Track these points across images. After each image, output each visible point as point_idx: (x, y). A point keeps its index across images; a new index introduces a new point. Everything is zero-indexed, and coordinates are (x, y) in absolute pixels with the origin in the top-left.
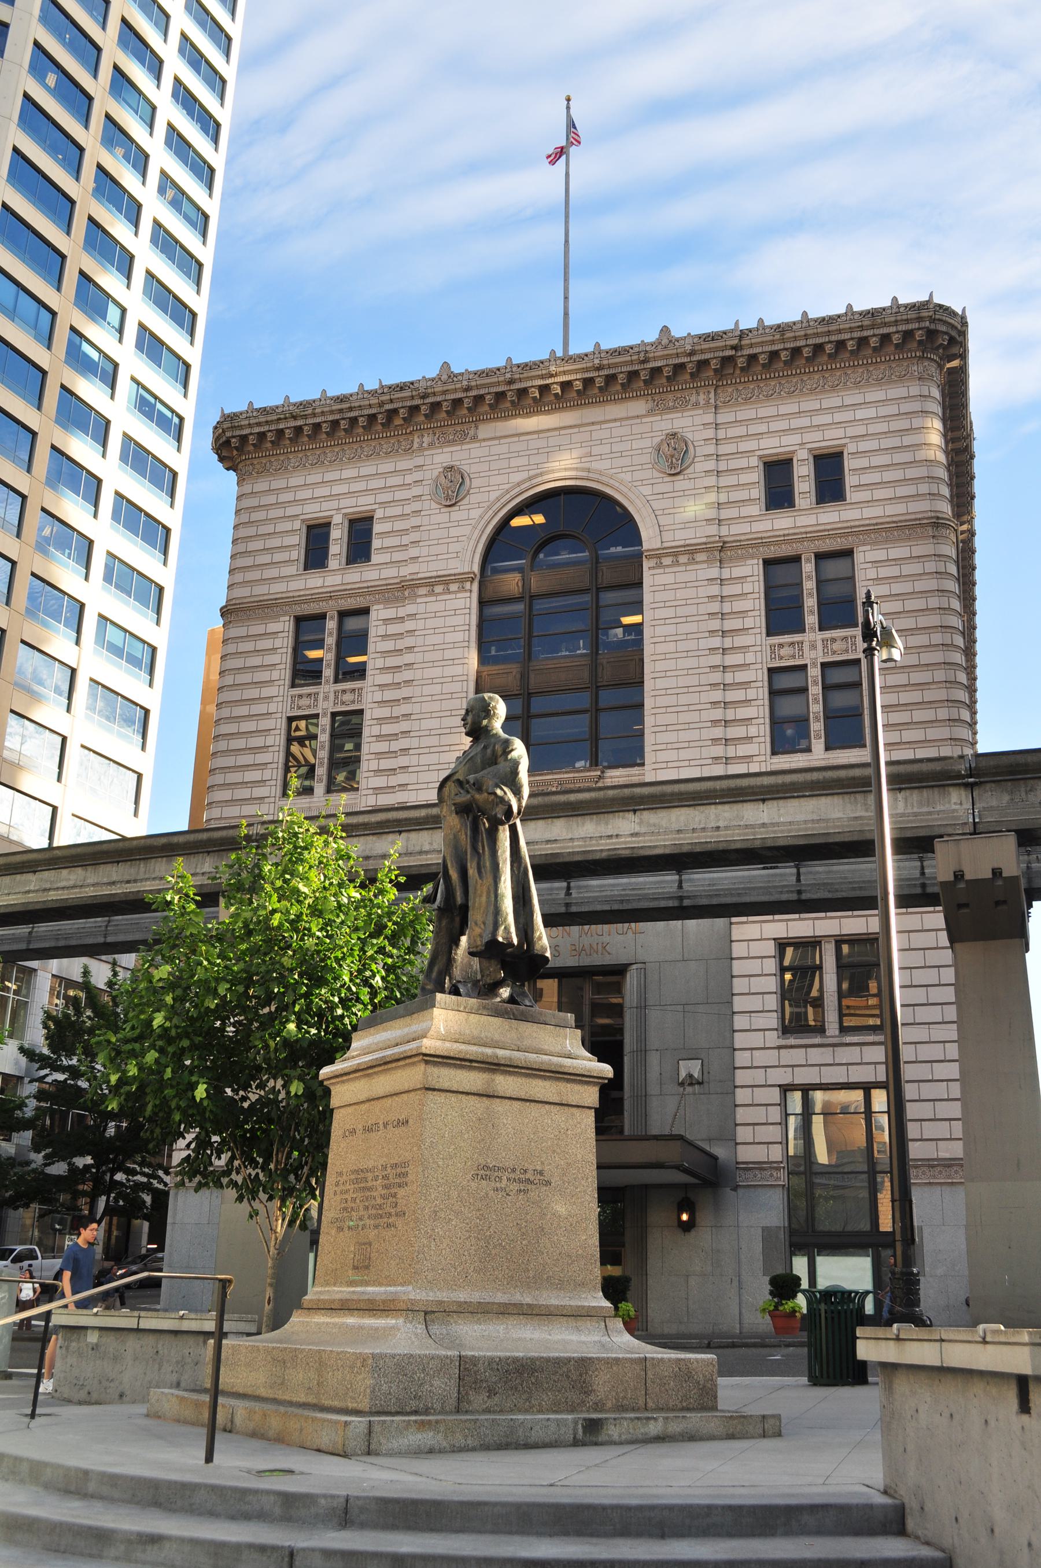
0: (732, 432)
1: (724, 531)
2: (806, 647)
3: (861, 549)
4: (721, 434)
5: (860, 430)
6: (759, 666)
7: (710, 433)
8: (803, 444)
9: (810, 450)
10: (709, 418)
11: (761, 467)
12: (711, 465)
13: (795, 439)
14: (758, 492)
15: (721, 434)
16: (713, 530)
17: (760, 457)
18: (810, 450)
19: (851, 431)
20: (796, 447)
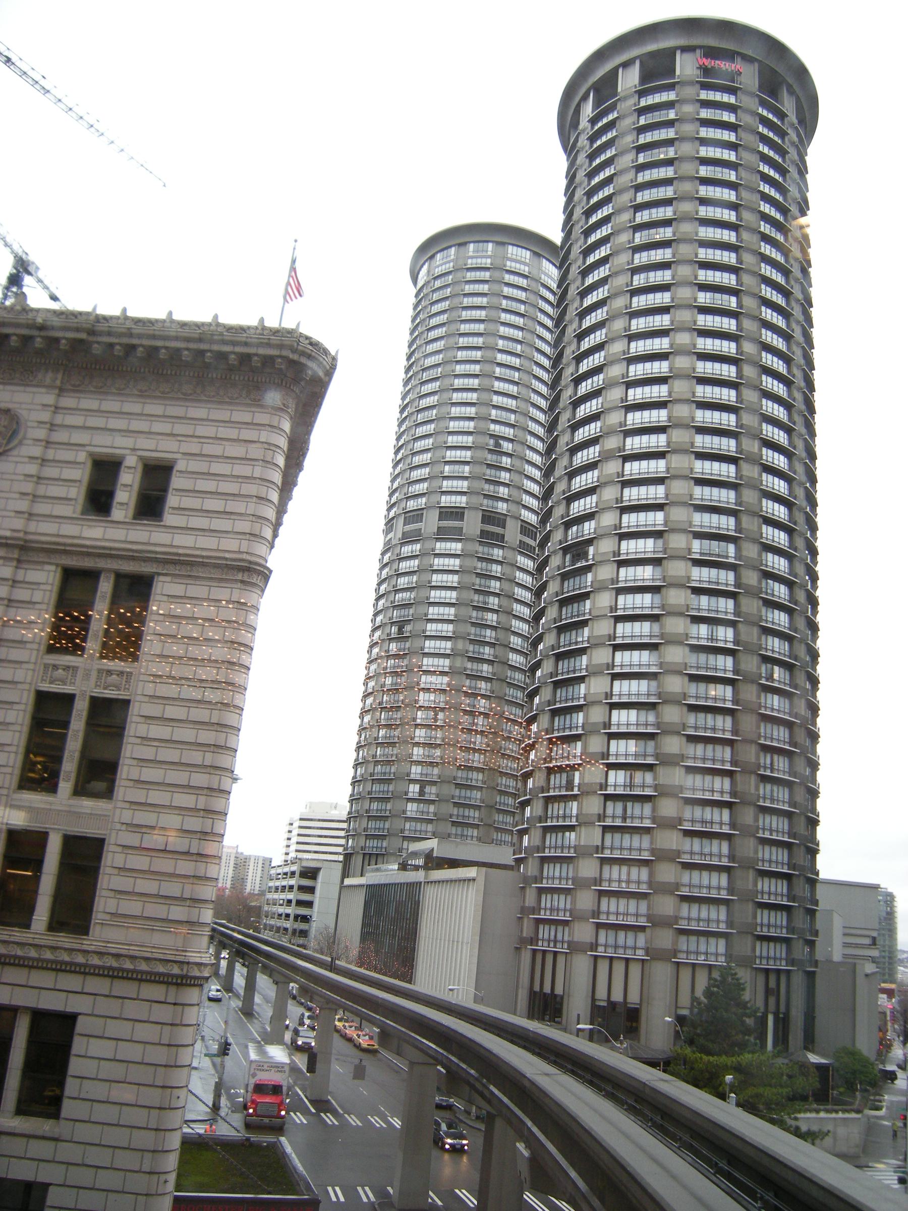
0: (70, 420)
1: (32, 527)
2: (80, 673)
3: (162, 578)
4: (59, 419)
5: (194, 448)
6: (27, 687)
7: (46, 416)
8: (134, 450)
9: (141, 458)
10: (50, 399)
11: (89, 465)
12: (37, 451)
13: (128, 442)
14: (78, 493)
15: (59, 419)
16: (18, 523)
17: (91, 454)
18: (141, 458)
19: (186, 447)
20: (127, 452)
